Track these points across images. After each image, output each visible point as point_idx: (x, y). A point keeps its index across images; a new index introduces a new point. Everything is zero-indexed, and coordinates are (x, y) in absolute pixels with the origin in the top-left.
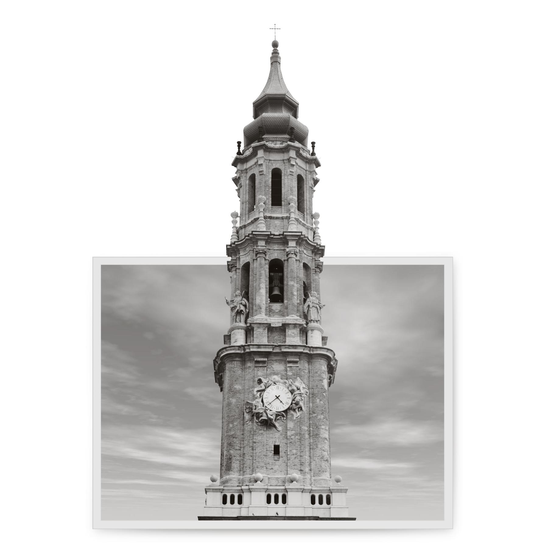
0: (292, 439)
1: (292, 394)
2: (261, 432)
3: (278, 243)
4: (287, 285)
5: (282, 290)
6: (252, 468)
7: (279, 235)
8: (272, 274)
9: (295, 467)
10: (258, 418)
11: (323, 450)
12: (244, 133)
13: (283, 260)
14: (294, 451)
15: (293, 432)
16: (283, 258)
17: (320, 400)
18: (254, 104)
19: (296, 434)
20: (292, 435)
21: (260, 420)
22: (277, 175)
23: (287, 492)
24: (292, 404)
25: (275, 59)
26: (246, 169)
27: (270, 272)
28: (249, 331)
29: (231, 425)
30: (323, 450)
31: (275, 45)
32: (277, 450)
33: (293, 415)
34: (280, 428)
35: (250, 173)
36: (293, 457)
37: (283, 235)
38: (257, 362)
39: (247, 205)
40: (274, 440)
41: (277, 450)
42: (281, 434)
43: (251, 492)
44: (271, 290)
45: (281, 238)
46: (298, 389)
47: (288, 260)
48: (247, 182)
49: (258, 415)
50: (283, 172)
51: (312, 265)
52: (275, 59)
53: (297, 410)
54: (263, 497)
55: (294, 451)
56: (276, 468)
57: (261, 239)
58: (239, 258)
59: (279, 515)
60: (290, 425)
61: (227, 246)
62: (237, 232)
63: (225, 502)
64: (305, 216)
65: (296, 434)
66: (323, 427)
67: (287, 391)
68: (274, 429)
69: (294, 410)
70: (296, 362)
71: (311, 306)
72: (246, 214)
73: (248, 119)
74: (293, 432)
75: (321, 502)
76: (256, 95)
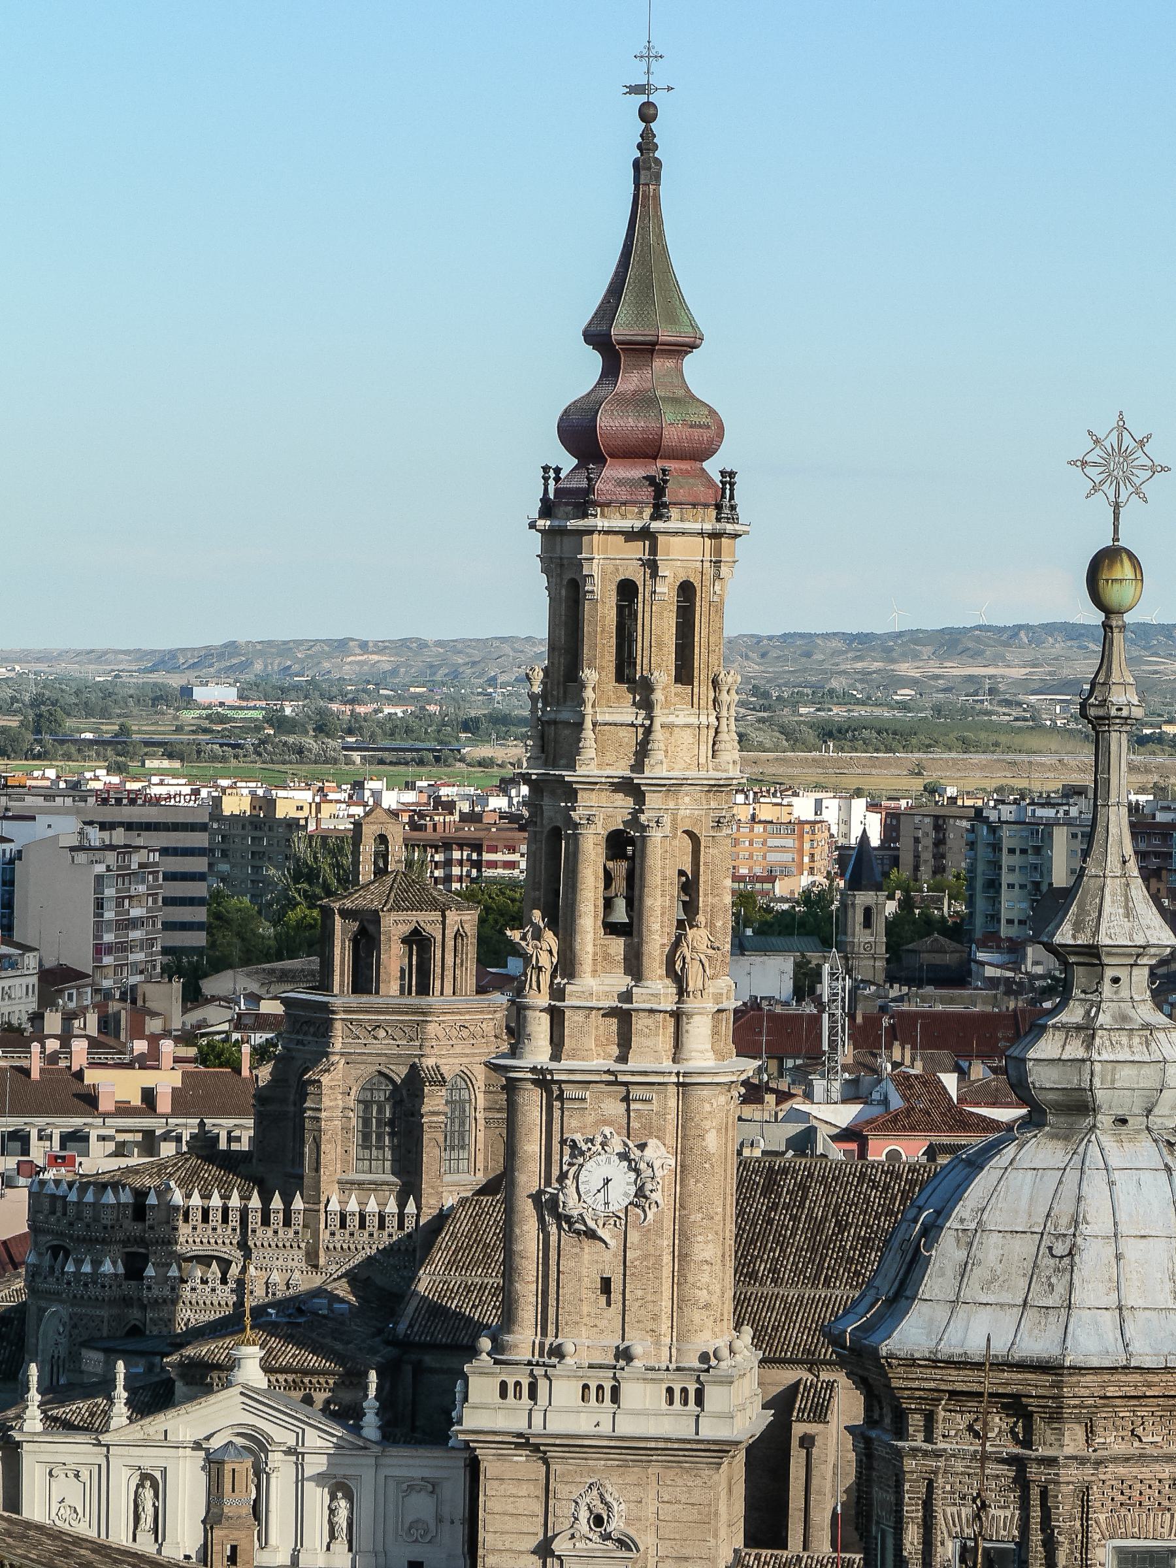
0: (635, 1267)
2: (575, 1250)
8: (610, 864)
9: (641, 1325)
11: (698, 1288)
12: (561, 419)
14: (639, 1293)
15: (639, 1252)
17: (697, 1181)
19: (646, 1257)
22: (627, 590)
25: (646, 167)
30: (698, 1288)
31: (647, 114)
34: (612, 1243)
39: (562, 660)
40: (601, 1266)
42: (615, 1256)
46: (650, 1165)
48: (563, 592)
52: (646, 167)
56: (602, 1324)
60: (634, 1237)
63: (503, 1394)
64: (696, 690)
66: (700, 1238)
70: (649, 1101)
71: (688, 960)
72: (558, 684)
74: (639, 1252)
75: (685, 1403)
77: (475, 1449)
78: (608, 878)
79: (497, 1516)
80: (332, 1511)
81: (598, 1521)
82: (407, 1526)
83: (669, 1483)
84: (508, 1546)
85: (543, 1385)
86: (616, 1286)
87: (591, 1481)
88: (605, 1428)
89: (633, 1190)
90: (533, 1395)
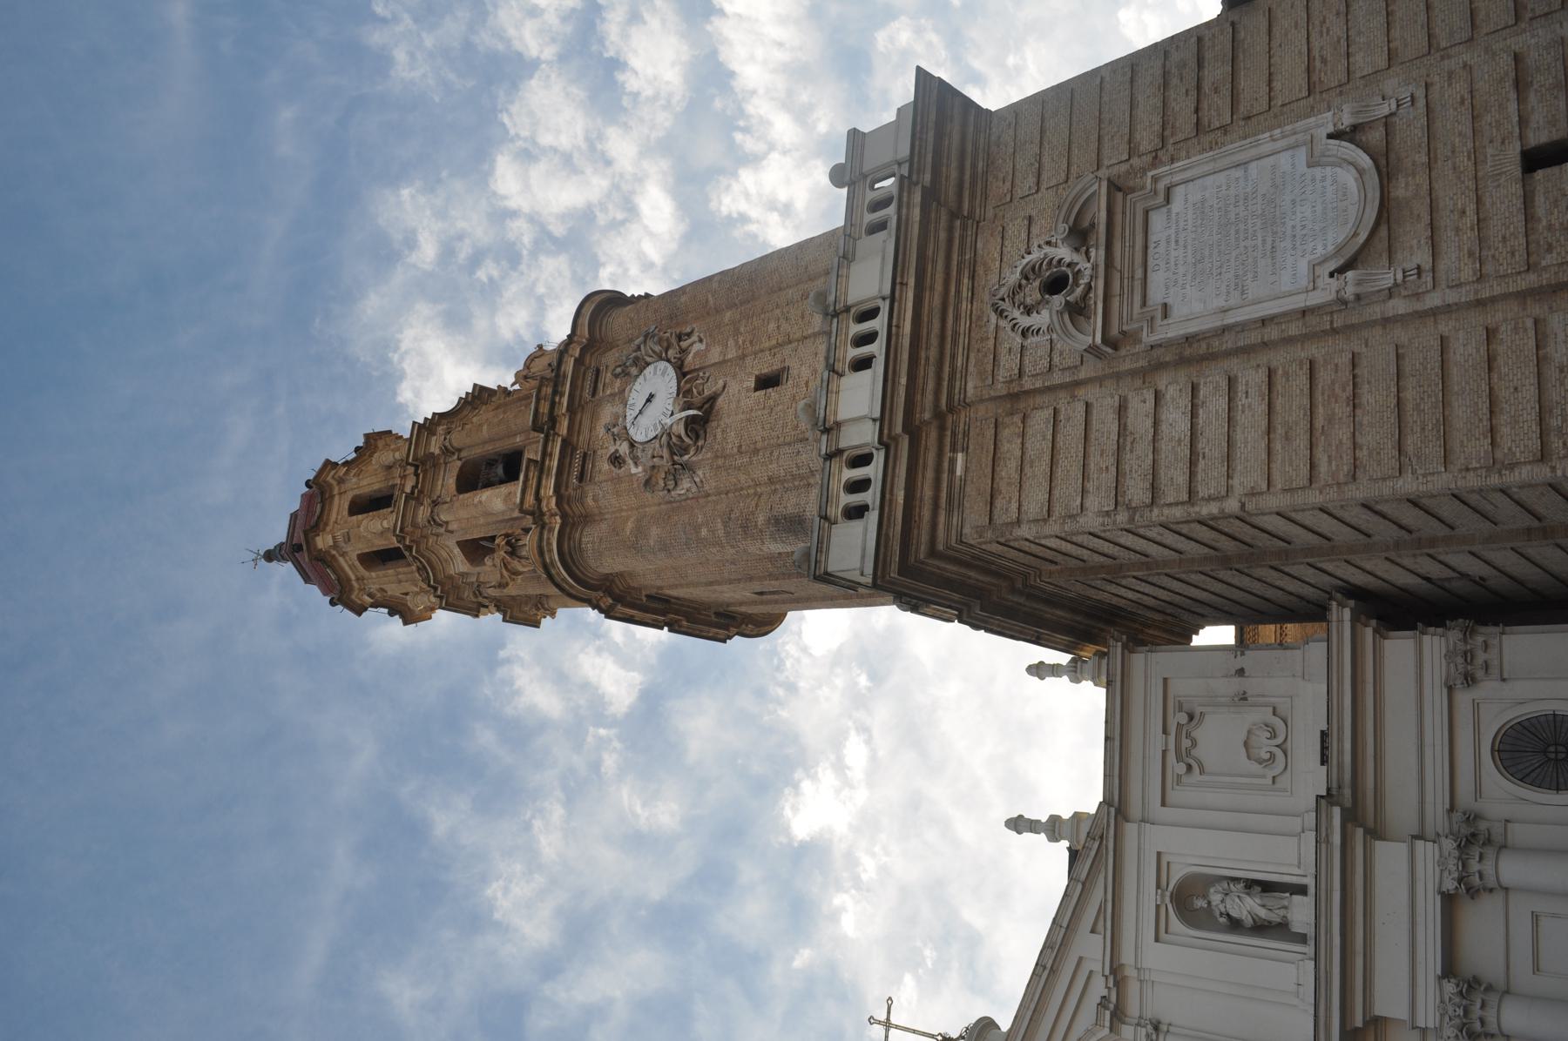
1: (648, 364)
2: (719, 436)
4: (491, 440)
6: (799, 446)
7: (417, 475)
10: (686, 450)
13: (459, 463)
14: (772, 326)
15: (731, 342)
20: (737, 342)
21: (687, 440)
23: (847, 309)
24: (668, 361)
29: (704, 532)
32: (767, 382)
33: (697, 353)
36: (785, 326)
38: (581, 478)
41: (767, 382)
42: (734, 376)
43: (838, 425)
45: (425, 472)
49: (676, 448)
50: (357, 492)
53: (684, 344)
55: (772, 326)
57: (415, 516)
60: (715, 355)
65: (737, 332)
67: (641, 379)
68: (720, 401)
69: (684, 351)
74: (731, 342)
77: (933, 552)
79: (1056, 493)
80: (1235, 925)
81: (1056, 285)
82: (1255, 768)
83: (1008, 184)
84: (1112, 460)
86: (766, 366)
87: (993, 317)
89: (663, 365)
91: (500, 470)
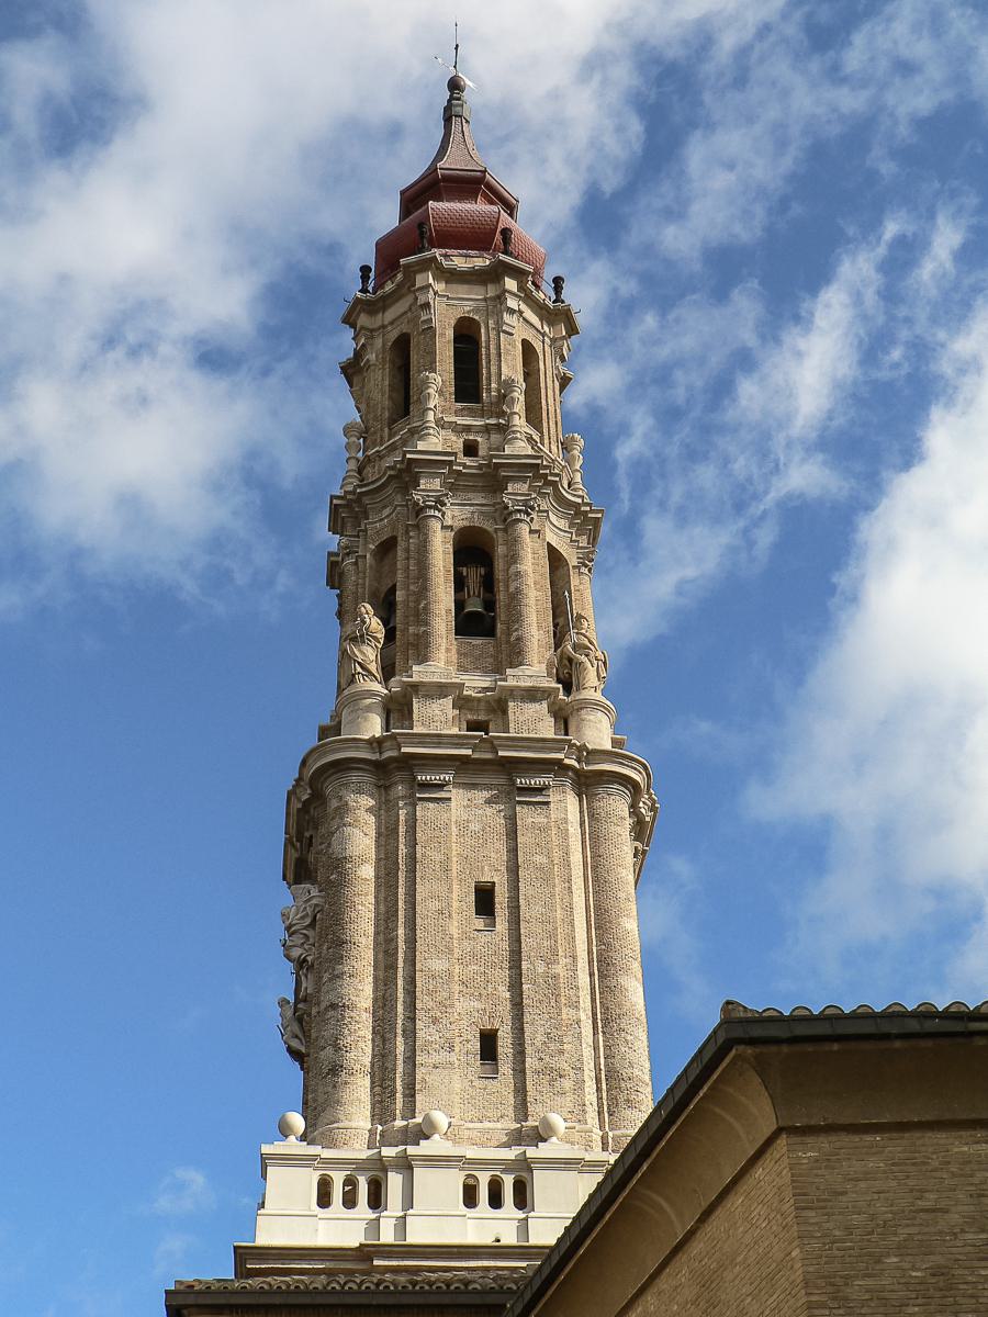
3: (473, 489)
5: (490, 605)
16: (488, 526)
18: (402, 193)
23: (531, 1171)
26: (384, 327)
27: (457, 564)
28: (397, 709)
32: (488, 1043)
35: (393, 335)
37: (488, 466)
44: (459, 605)
47: (505, 530)
51: (571, 557)
54: (455, 1180)
58: (366, 531)
59: (502, 1243)
61: (332, 497)
62: (360, 471)
63: (324, 1200)
73: (387, 218)
76: (411, 174)
78: (460, 583)
85: (394, 1181)
86: (505, 1046)
88: (510, 1238)
90: (376, 1201)
91: (474, 606)
